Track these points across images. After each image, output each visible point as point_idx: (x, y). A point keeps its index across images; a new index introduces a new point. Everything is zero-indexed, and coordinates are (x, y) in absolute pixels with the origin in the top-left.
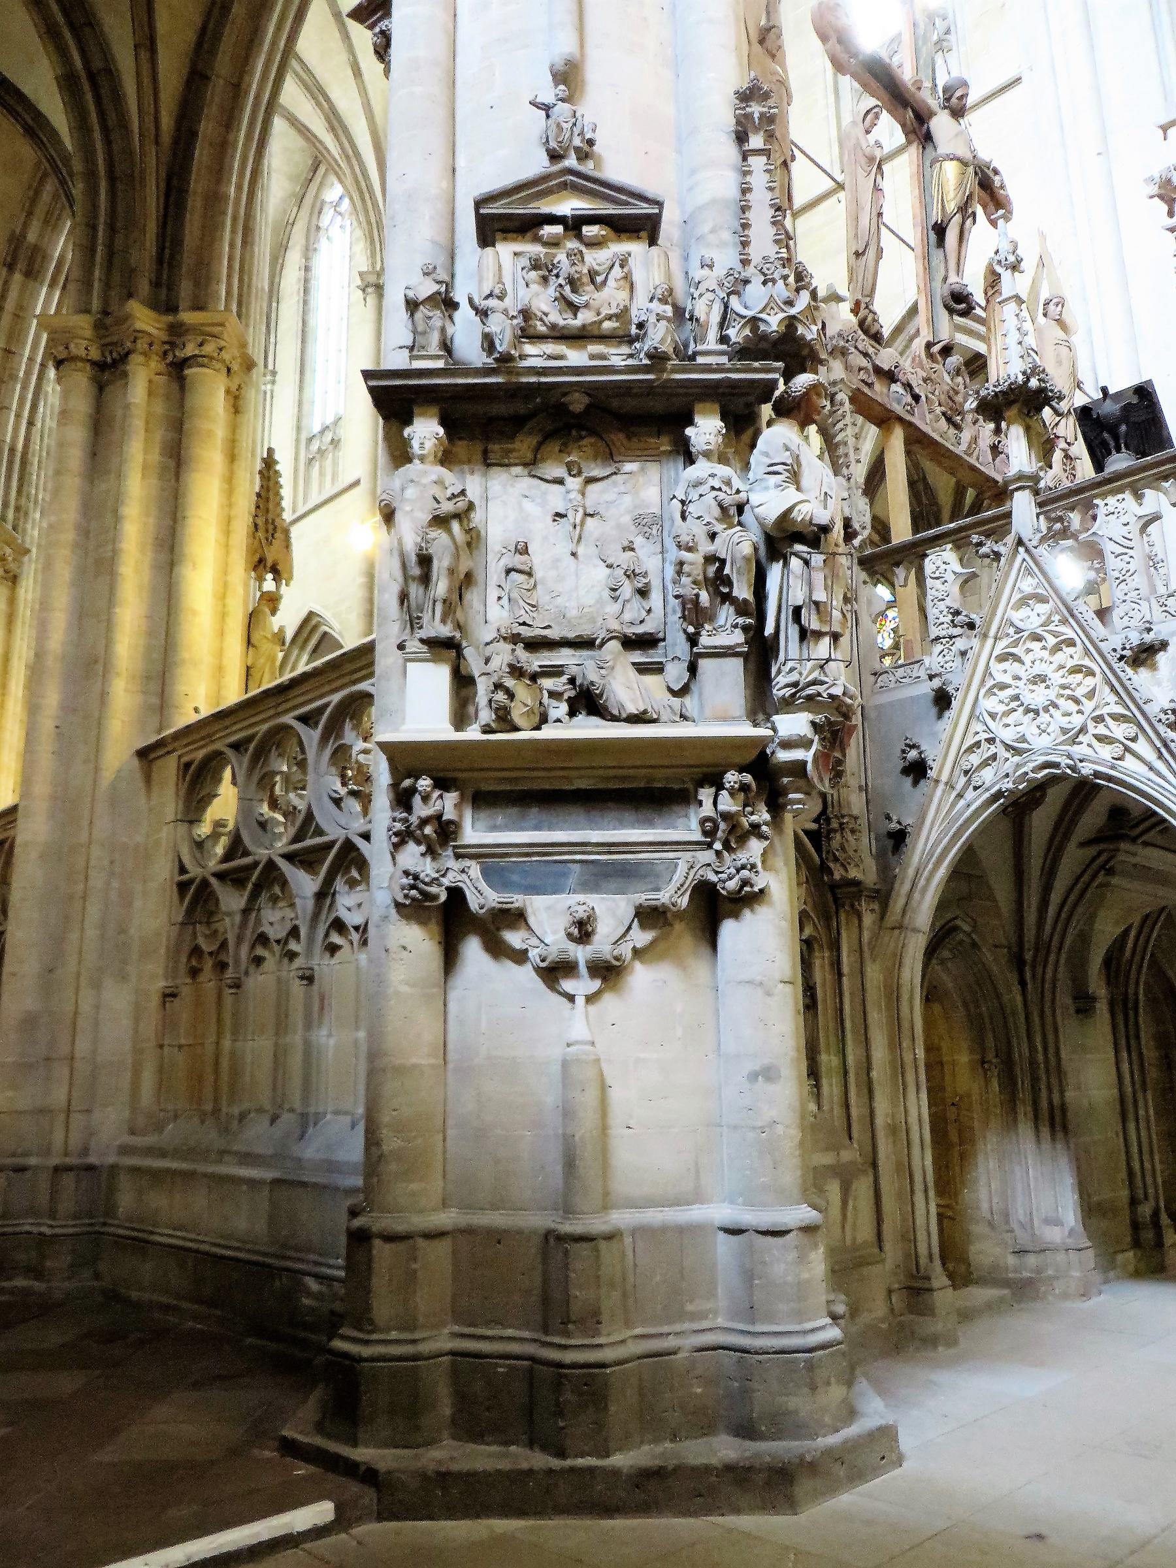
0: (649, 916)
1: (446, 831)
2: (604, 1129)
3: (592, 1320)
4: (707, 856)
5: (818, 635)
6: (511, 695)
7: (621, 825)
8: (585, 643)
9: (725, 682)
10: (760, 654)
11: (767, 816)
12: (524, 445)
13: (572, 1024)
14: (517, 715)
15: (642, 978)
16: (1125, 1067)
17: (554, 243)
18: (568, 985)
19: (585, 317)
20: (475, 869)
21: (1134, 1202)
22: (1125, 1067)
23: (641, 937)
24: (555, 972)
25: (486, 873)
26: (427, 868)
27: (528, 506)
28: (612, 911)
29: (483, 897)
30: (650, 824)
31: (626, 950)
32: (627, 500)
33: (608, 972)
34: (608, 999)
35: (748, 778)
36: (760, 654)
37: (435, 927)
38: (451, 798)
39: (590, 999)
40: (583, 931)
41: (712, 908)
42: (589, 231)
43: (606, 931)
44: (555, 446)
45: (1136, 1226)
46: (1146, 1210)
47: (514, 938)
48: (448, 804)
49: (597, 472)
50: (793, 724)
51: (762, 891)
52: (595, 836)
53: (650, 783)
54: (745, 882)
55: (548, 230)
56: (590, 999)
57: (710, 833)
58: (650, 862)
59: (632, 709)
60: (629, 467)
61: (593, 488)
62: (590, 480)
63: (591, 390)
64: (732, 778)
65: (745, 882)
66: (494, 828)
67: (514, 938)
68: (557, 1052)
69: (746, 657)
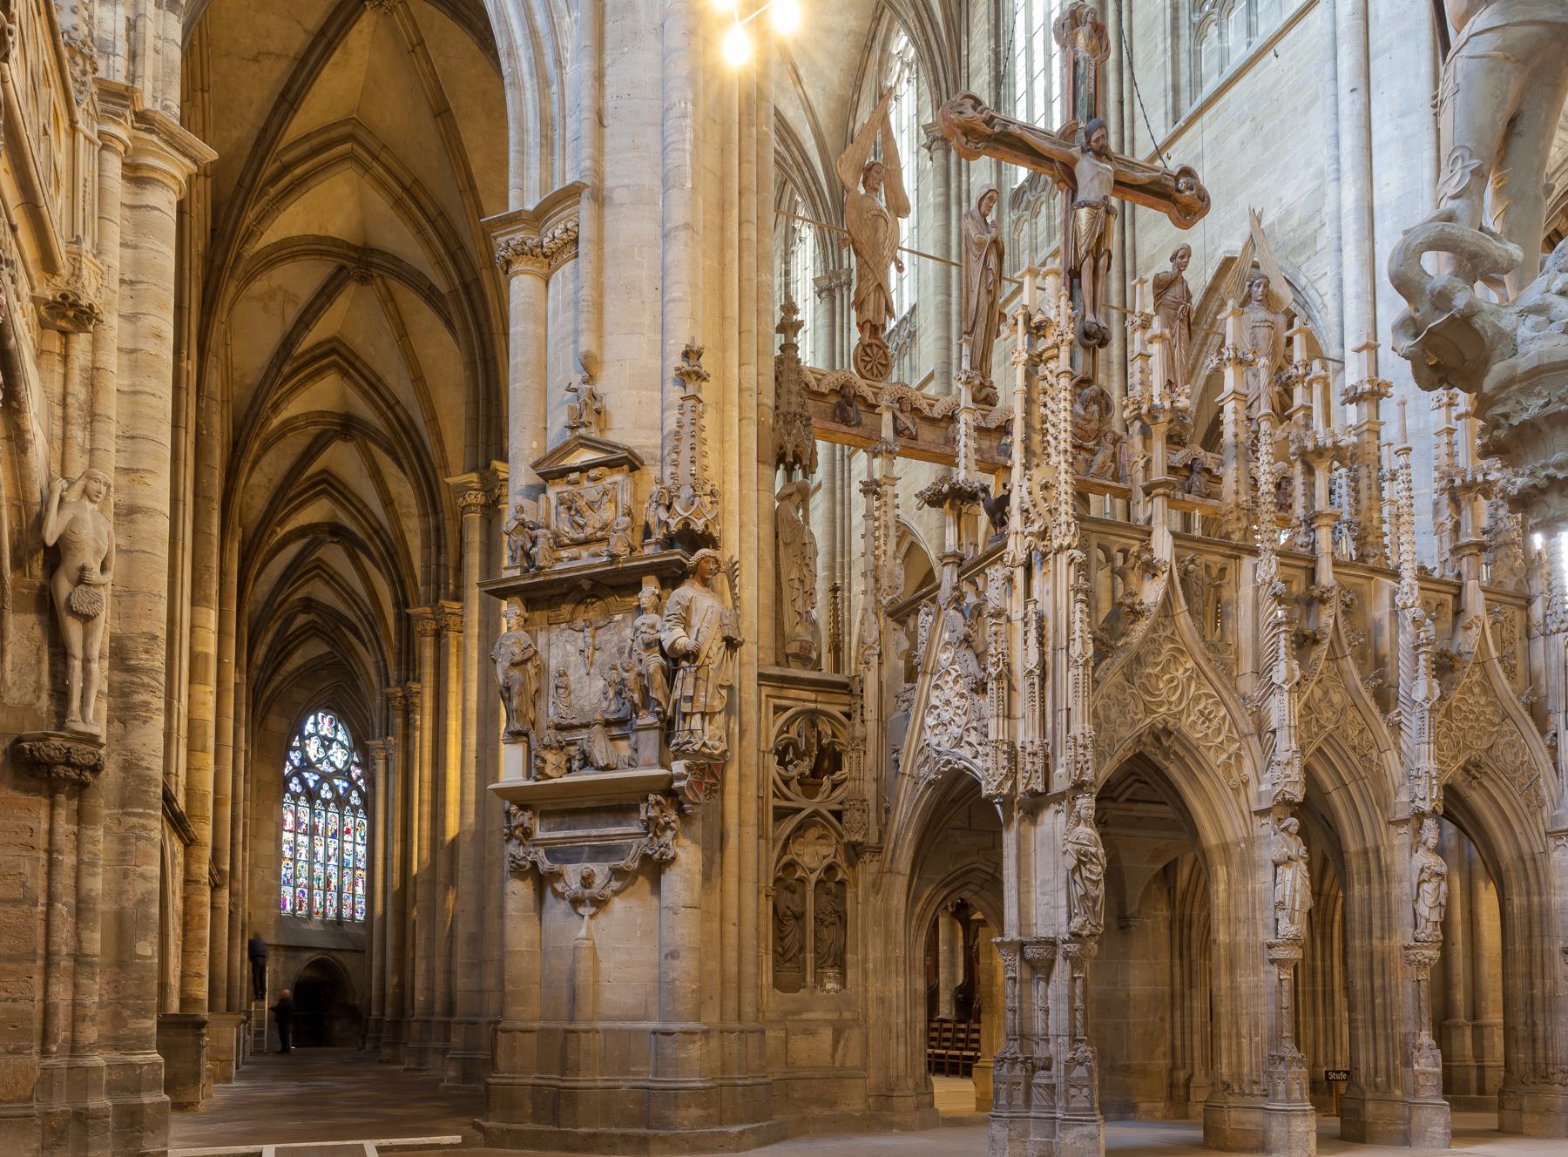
0: (617, 873)
1: (527, 833)
2: (596, 982)
3: (576, 1068)
4: (645, 841)
5: (692, 714)
6: (544, 761)
7: (608, 825)
8: (587, 726)
9: (649, 743)
10: (667, 727)
11: (674, 817)
12: (566, 609)
13: (582, 928)
14: (548, 770)
15: (618, 905)
17: (577, 483)
18: (581, 910)
19: (589, 530)
20: (542, 852)
21: (1173, 1068)
23: (615, 885)
24: (576, 902)
25: (547, 853)
26: (520, 852)
27: (569, 647)
28: (600, 870)
29: (546, 865)
30: (620, 824)
31: (608, 892)
32: (616, 638)
33: (600, 903)
34: (601, 916)
35: (659, 798)
36: (667, 727)
37: (529, 881)
38: (528, 814)
39: (591, 917)
40: (587, 881)
41: (655, 868)
42: (593, 473)
43: (599, 880)
44: (582, 608)
45: (1172, 1086)
46: (1181, 1075)
47: (559, 887)
48: (525, 818)
49: (601, 623)
50: (678, 767)
51: (674, 859)
52: (594, 832)
53: (617, 803)
54: (662, 854)
55: (573, 476)
56: (591, 917)
57: (647, 828)
58: (620, 845)
59: (601, 764)
60: (618, 617)
61: (600, 632)
62: (597, 628)
63: (589, 577)
64: (652, 797)
65: (662, 854)
66: (549, 830)
67: (559, 887)
68: (572, 944)
69: (661, 729)
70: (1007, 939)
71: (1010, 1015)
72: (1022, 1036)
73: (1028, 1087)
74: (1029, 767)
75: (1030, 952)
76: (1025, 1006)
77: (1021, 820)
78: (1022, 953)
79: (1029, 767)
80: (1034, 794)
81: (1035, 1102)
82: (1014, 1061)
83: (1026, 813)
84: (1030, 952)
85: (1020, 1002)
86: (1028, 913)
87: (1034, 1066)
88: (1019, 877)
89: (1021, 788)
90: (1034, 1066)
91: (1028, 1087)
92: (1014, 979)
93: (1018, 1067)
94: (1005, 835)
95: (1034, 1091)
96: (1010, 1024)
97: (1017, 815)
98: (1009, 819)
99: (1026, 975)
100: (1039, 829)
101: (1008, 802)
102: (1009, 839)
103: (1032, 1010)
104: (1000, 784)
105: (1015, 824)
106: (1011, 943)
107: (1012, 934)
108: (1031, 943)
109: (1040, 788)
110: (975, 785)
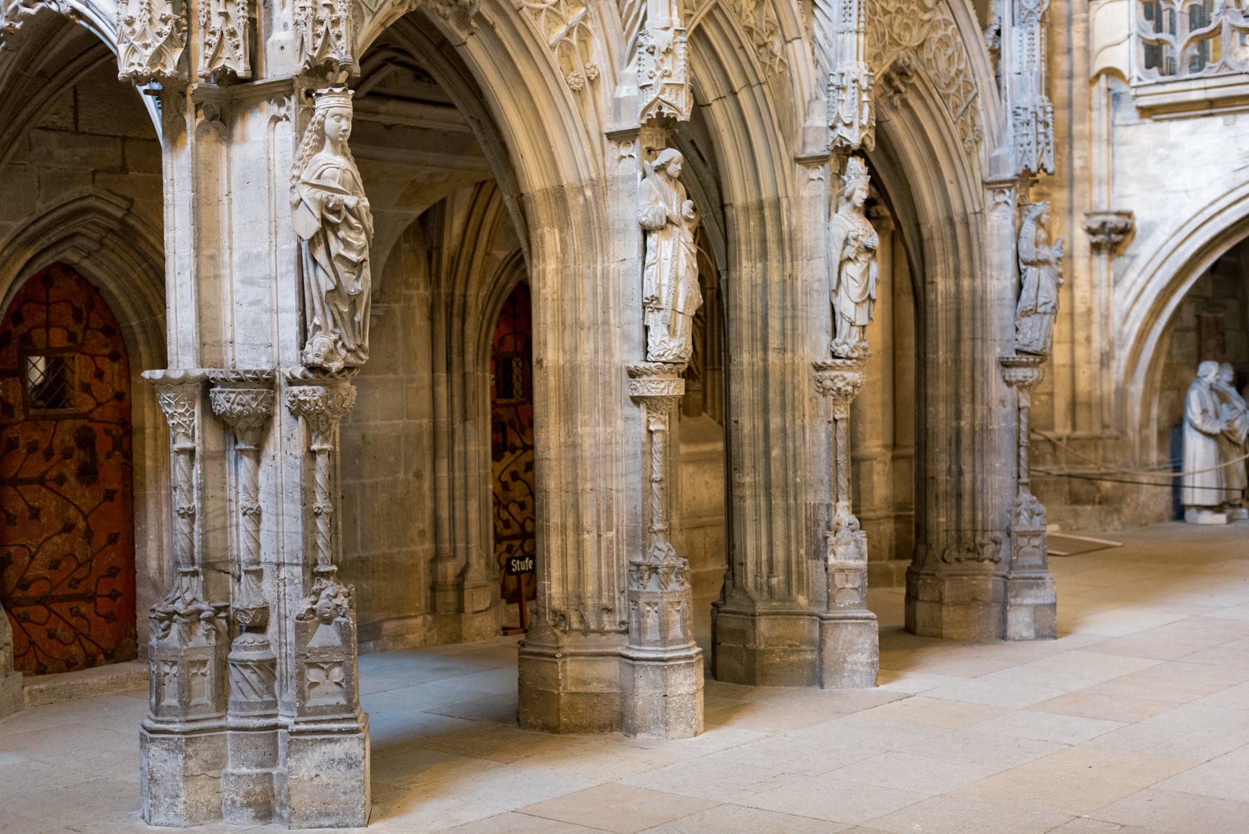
16: (442, 390)
22: (442, 390)
70: (175, 372)
71: (181, 524)
72: (208, 565)
73: (223, 665)
74: (217, 23)
75: (223, 400)
76: (212, 505)
77: (201, 131)
78: (207, 401)
79: (217, 23)
80: (227, 78)
81: (235, 696)
82: (194, 617)
83: (212, 118)
84: (223, 400)
85: (203, 499)
86: (217, 320)
87: (231, 622)
88: (197, 248)
89: (201, 66)
90: (231, 622)
91: (223, 665)
92: (191, 453)
93: (202, 628)
94: (167, 160)
95: (234, 675)
96: (182, 542)
97: (192, 121)
98: (175, 128)
99: (214, 444)
100: (237, 151)
101: (173, 93)
102: (177, 170)
103: (225, 513)
104: (159, 55)
105: (190, 138)
106: (182, 382)
107: (183, 361)
108: (225, 382)
109: (241, 69)
110: (108, 58)
